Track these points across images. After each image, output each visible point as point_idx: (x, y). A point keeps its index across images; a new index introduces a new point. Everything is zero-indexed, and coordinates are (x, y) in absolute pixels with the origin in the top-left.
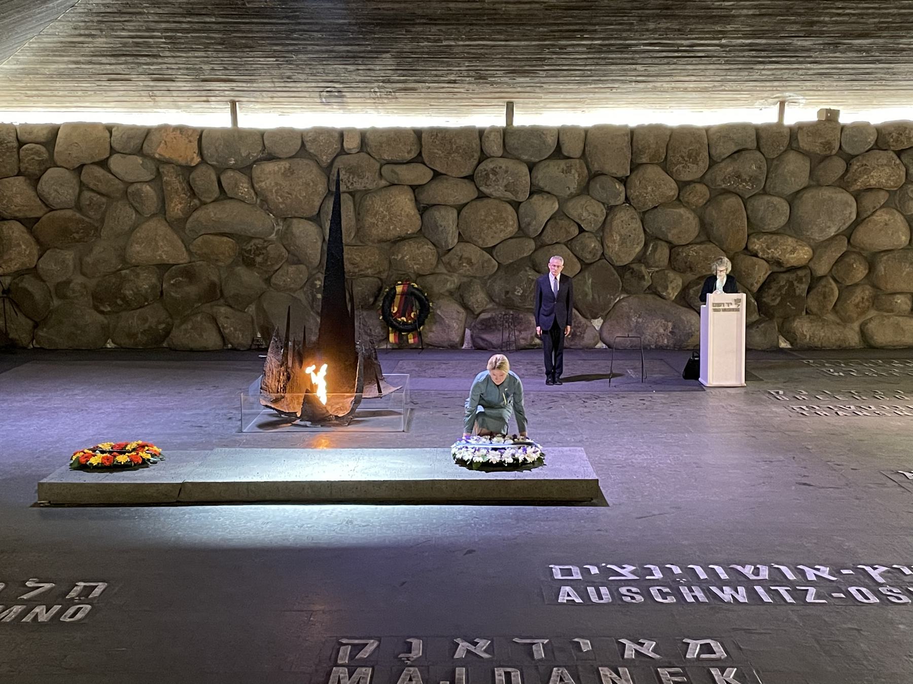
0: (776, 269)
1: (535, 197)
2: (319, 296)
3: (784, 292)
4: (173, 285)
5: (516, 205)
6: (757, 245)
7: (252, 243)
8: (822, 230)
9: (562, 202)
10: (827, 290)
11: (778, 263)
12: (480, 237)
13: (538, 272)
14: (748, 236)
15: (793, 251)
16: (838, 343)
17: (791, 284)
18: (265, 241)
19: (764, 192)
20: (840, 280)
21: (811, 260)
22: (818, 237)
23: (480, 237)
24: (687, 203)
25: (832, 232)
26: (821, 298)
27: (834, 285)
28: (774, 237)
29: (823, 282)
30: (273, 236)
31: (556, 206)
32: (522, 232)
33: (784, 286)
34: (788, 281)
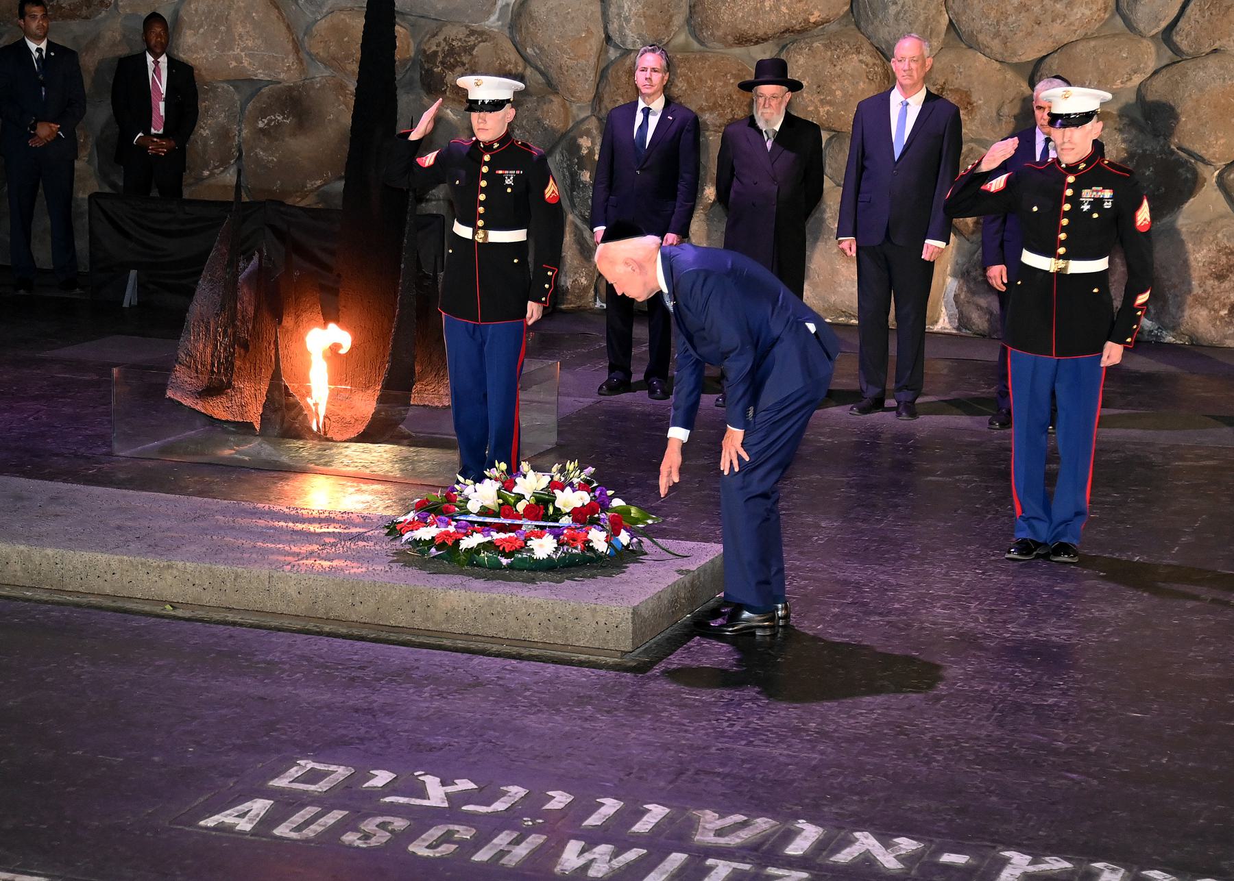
2: (586, 176)
4: (261, 129)
7: (440, 38)
12: (997, 34)
18: (473, 32)
23: (997, 34)
30: (493, 22)
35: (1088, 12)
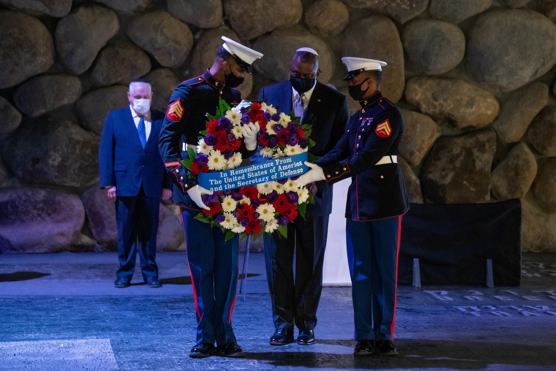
0: (448, 131)
1: (82, 11)
3: (458, 164)
5: (51, 23)
6: (419, 93)
8: (511, 73)
9: (126, 21)
10: (520, 163)
11: (449, 121)
13: (87, 129)
14: (407, 80)
15: (471, 104)
16: (538, 242)
17: (469, 152)
19: (429, 15)
20: (539, 149)
21: (497, 118)
22: (510, 84)
24: (316, 28)
25: (526, 75)
26: (512, 174)
27: (532, 159)
28: (444, 82)
29: (515, 152)
31: (115, 27)
32: (60, 66)
33: (458, 155)
34: (464, 148)
35: (44, 60)
